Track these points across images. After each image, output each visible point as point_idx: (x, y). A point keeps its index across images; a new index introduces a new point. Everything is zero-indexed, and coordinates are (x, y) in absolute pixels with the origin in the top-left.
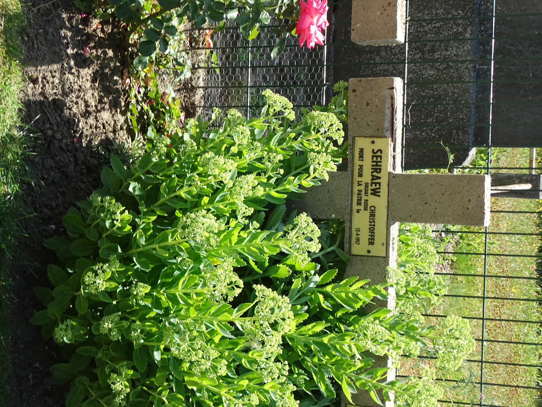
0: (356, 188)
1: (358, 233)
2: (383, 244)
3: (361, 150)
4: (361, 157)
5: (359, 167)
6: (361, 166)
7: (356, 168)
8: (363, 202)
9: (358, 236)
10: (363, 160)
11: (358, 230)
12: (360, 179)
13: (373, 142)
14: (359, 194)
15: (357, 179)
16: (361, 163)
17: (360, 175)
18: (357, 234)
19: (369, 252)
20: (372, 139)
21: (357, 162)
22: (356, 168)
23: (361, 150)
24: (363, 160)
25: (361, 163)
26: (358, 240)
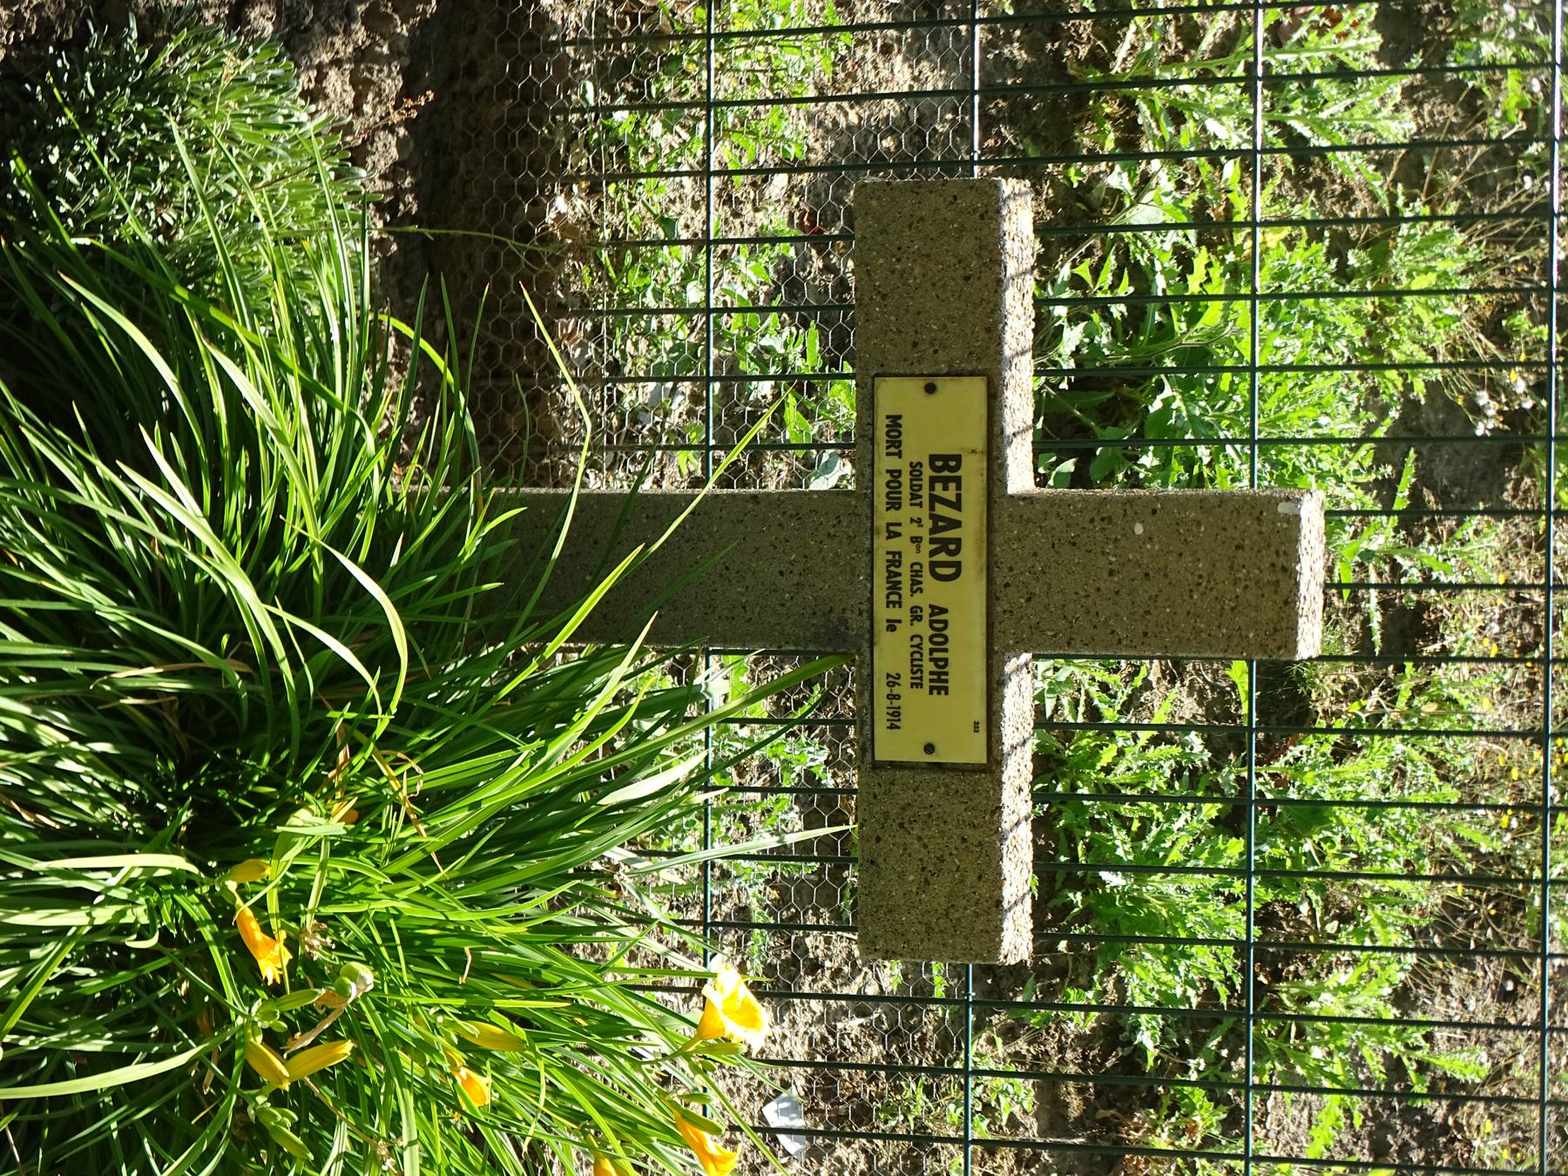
0: (882, 545)
1: (896, 690)
2: (976, 724)
3: (895, 422)
4: (895, 443)
5: (888, 477)
7: (881, 481)
9: (896, 703)
10: (899, 455)
13: (930, 389)
14: (891, 563)
15: (883, 516)
18: (893, 697)
19: (929, 748)
20: (929, 380)
21: (885, 463)
22: (881, 481)
24: (899, 455)
26: (895, 714)
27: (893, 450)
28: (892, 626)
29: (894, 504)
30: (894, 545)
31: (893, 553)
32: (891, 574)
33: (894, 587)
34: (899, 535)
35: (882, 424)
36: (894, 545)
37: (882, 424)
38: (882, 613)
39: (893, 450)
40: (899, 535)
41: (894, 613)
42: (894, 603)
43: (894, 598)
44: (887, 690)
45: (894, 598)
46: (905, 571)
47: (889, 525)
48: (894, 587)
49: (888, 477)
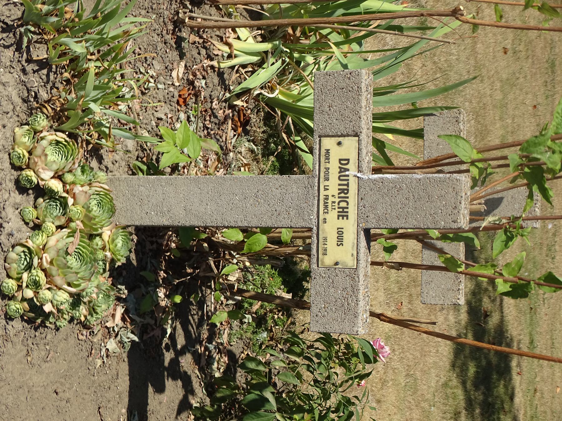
0: (323, 193)
3: (328, 151)
4: (327, 158)
5: (325, 170)
6: (327, 169)
8: (330, 209)
9: (325, 246)
10: (329, 162)
11: (325, 239)
12: (327, 183)
17: (327, 179)
19: (337, 264)
20: (340, 139)
25: (328, 165)
26: (326, 250)
27: (327, 161)
30: (326, 193)
31: (326, 196)
32: (325, 203)
33: (326, 207)
35: (323, 152)
36: (326, 193)
37: (323, 152)
39: (327, 161)
41: (326, 216)
42: (326, 212)
43: (326, 211)
45: (326, 211)
48: (326, 207)
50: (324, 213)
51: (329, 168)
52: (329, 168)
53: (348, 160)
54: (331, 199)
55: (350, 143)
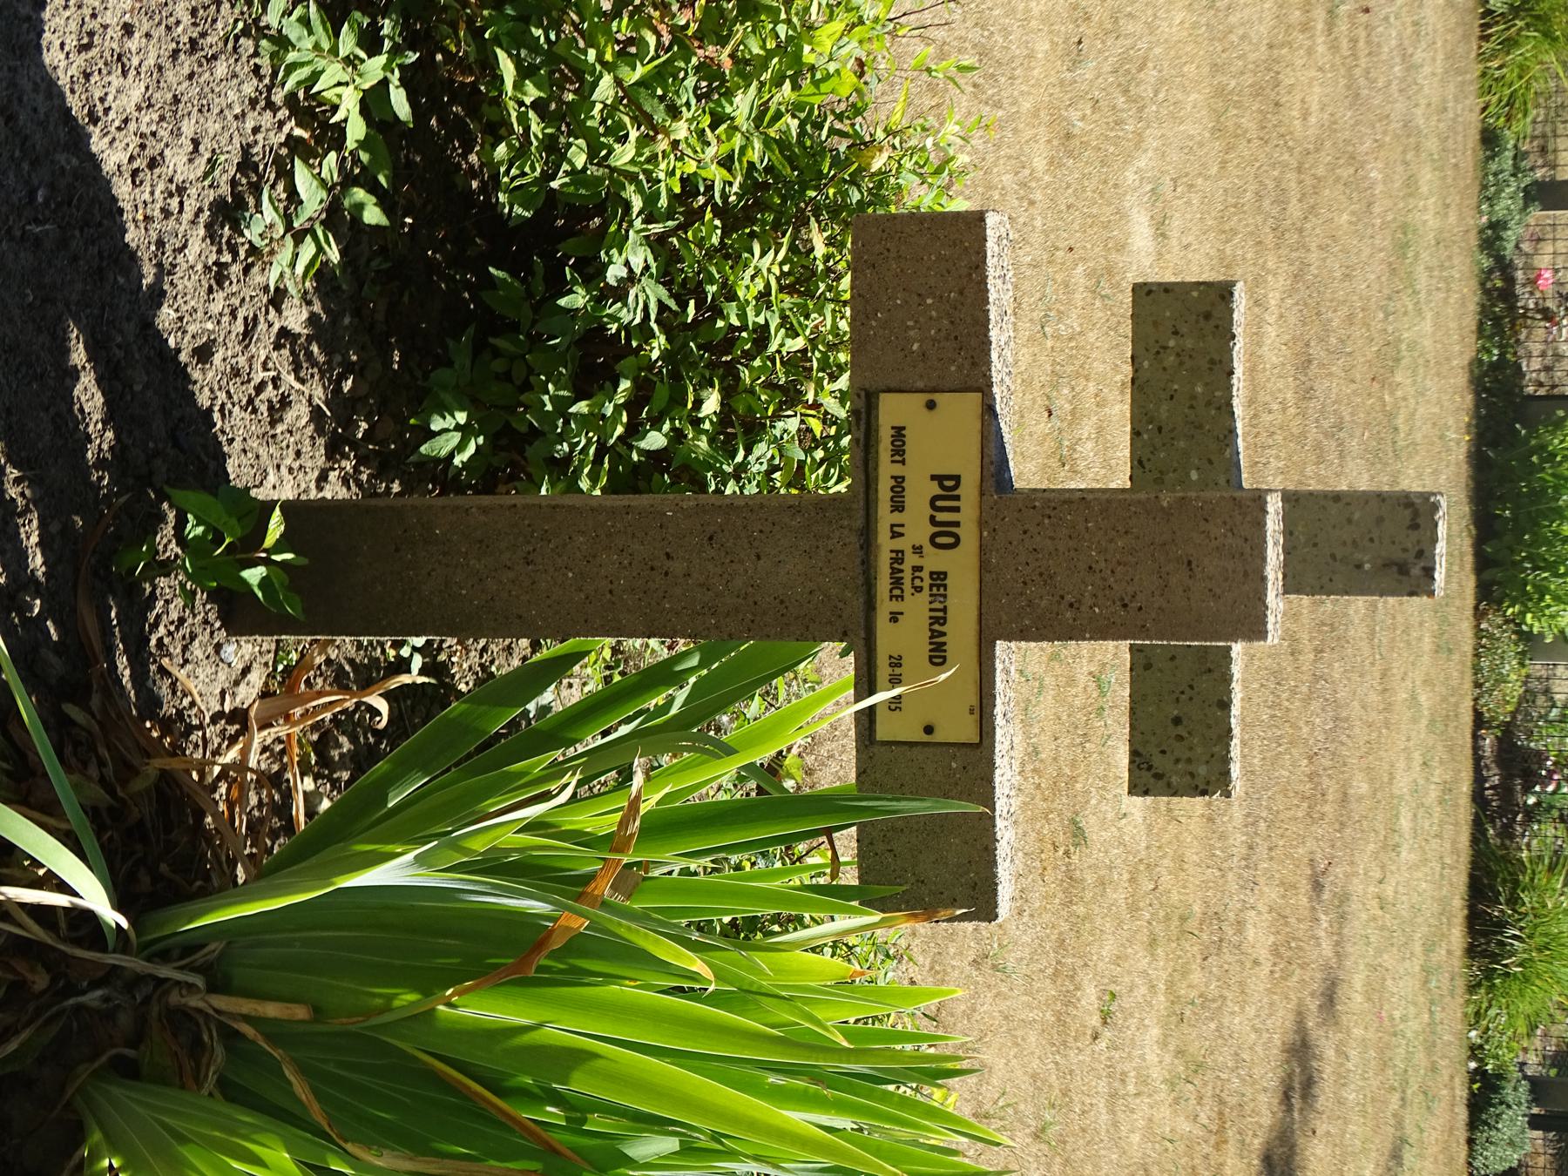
0: (885, 544)
3: (899, 432)
4: (899, 451)
5: (893, 483)
6: (899, 480)
10: (903, 462)
11: (896, 662)
12: (897, 518)
15: (885, 517)
16: (897, 470)
17: (898, 507)
19: (929, 730)
21: (886, 469)
23: (899, 432)
24: (903, 462)
25: (897, 470)
28: (894, 617)
29: (898, 507)
30: (898, 544)
31: (897, 552)
32: (894, 571)
34: (902, 535)
36: (898, 544)
38: (885, 607)
39: (897, 458)
40: (902, 535)
41: (895, 606)
44: (890, 670)
46: (907, 567)
47: (892, 526)
48: (897, 582)
49: (893, 483)
50: (891, 597)
51: (903, 478)
52: (903, 478)
53: (957, 478)
54: (911, 560)
55: (960, 408)
